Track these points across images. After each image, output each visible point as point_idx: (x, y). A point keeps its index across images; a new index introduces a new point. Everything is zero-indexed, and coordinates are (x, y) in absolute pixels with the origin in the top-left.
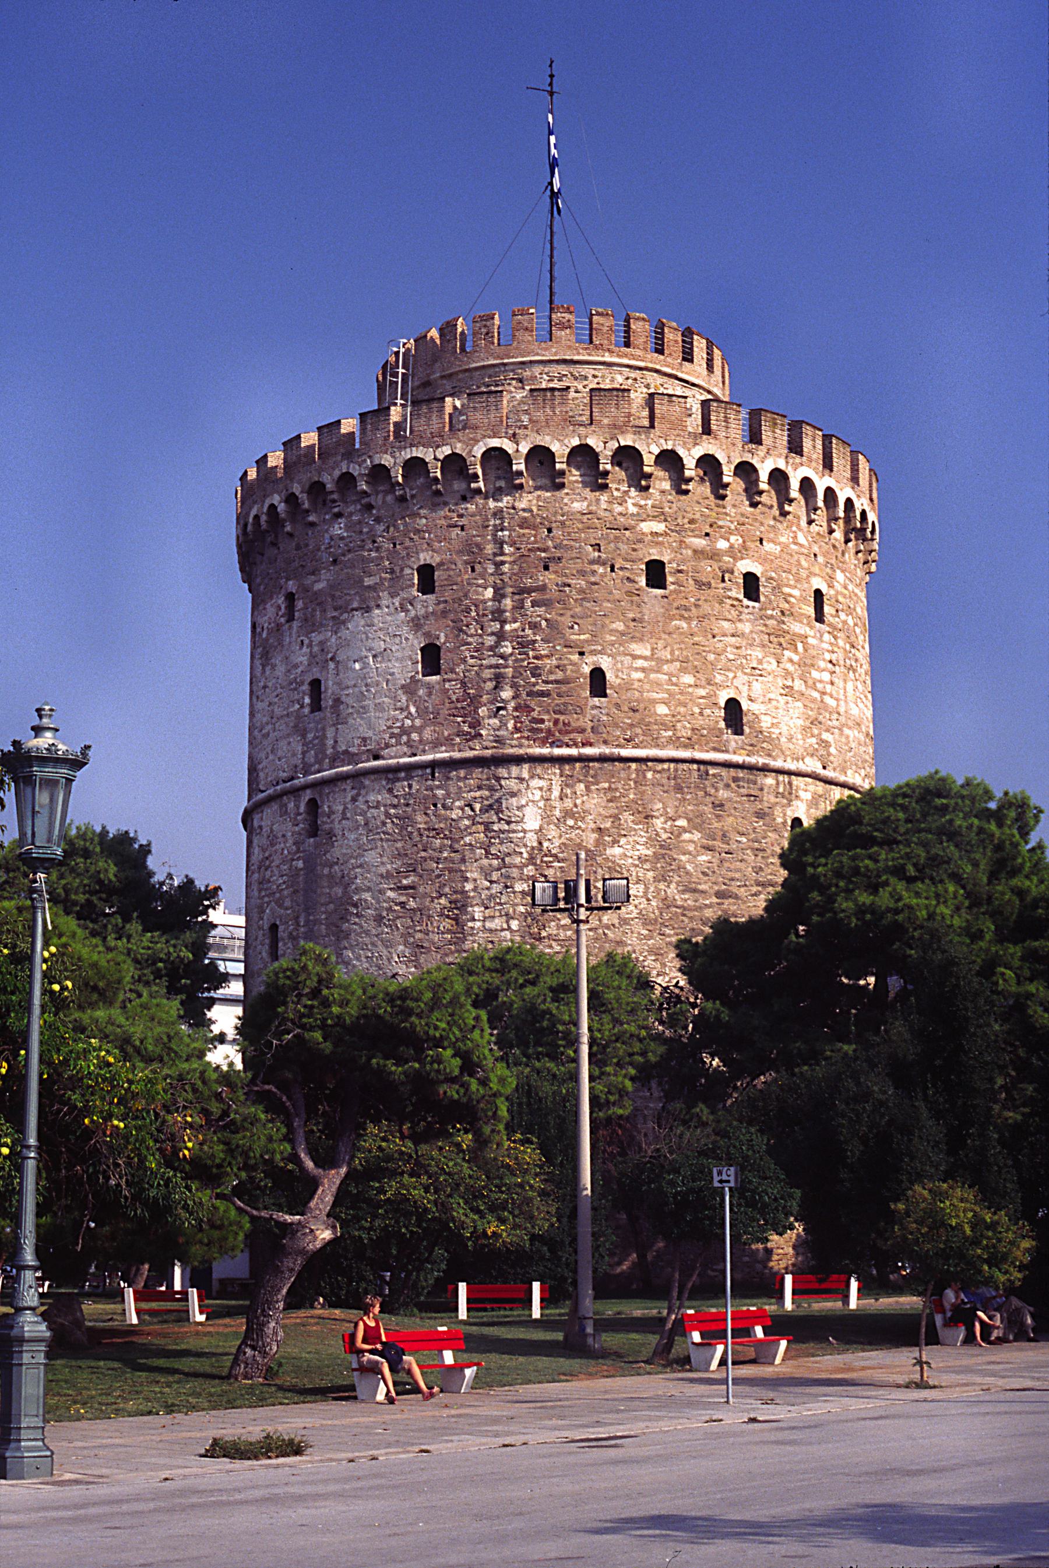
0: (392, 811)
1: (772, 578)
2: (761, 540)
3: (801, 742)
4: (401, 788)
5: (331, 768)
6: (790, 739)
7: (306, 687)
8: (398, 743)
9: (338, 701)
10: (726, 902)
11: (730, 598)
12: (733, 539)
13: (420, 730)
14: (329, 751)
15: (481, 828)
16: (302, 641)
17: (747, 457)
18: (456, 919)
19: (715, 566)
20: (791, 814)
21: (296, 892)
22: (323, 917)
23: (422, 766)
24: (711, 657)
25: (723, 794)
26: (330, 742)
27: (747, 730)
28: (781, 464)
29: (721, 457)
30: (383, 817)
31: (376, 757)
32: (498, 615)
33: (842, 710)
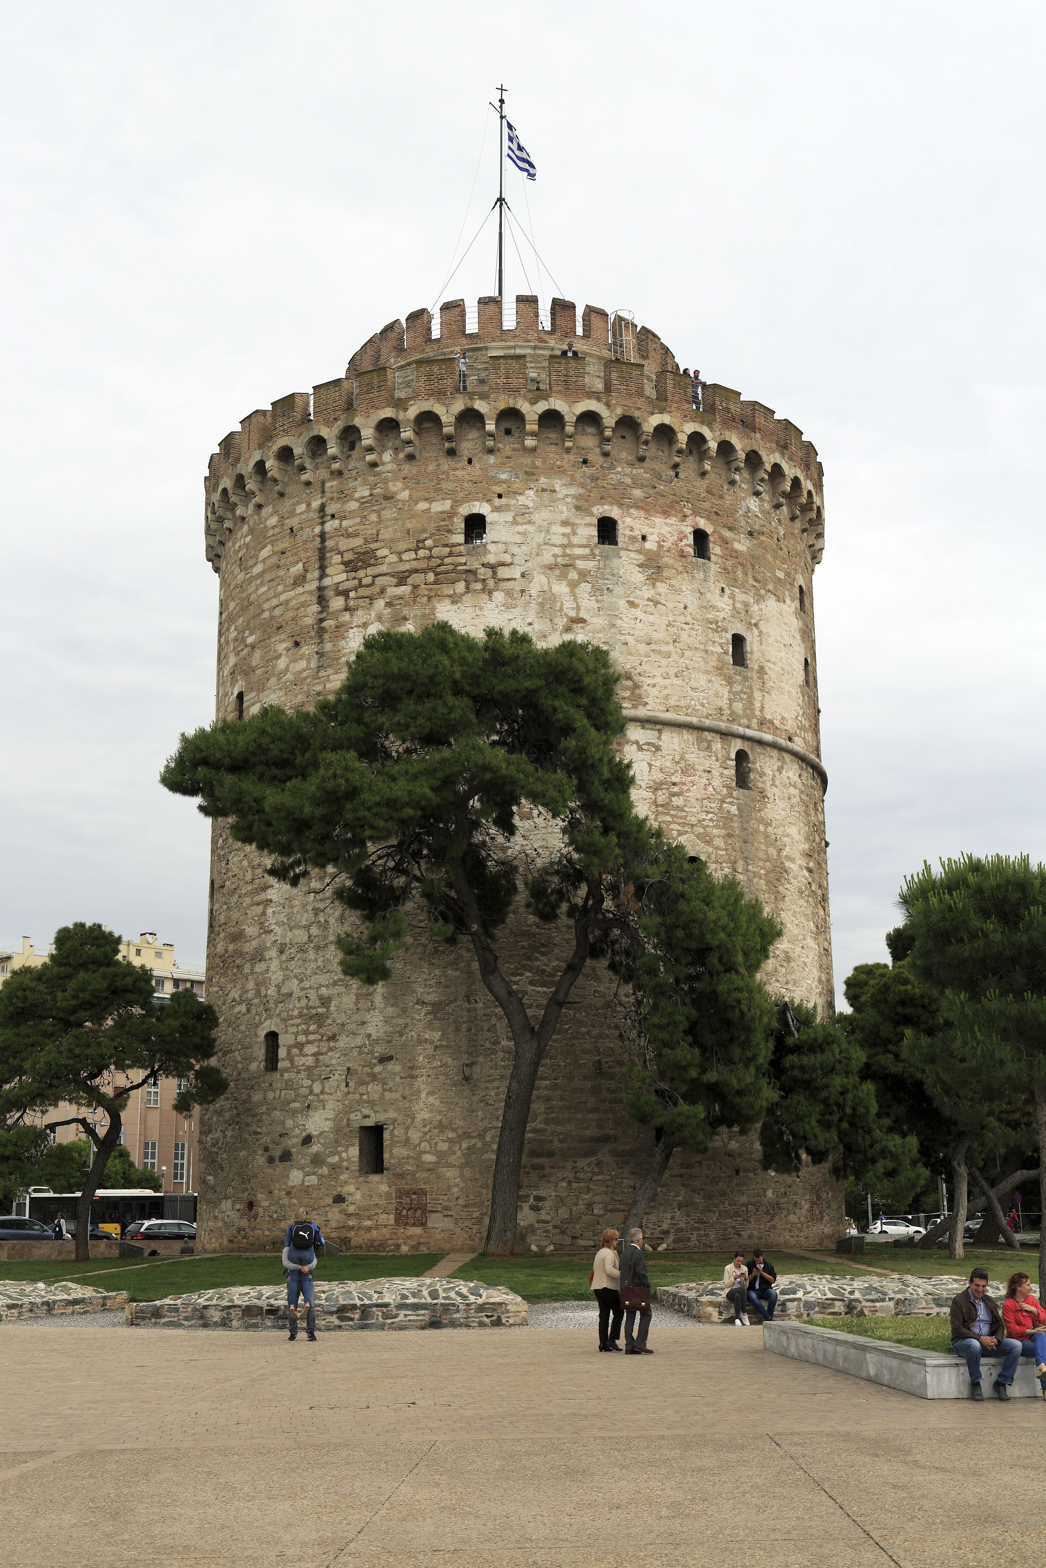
9: (761, 670)
14: (758, 713)
16: (723, 590)
26: (758, 705)
31: (790, 739)
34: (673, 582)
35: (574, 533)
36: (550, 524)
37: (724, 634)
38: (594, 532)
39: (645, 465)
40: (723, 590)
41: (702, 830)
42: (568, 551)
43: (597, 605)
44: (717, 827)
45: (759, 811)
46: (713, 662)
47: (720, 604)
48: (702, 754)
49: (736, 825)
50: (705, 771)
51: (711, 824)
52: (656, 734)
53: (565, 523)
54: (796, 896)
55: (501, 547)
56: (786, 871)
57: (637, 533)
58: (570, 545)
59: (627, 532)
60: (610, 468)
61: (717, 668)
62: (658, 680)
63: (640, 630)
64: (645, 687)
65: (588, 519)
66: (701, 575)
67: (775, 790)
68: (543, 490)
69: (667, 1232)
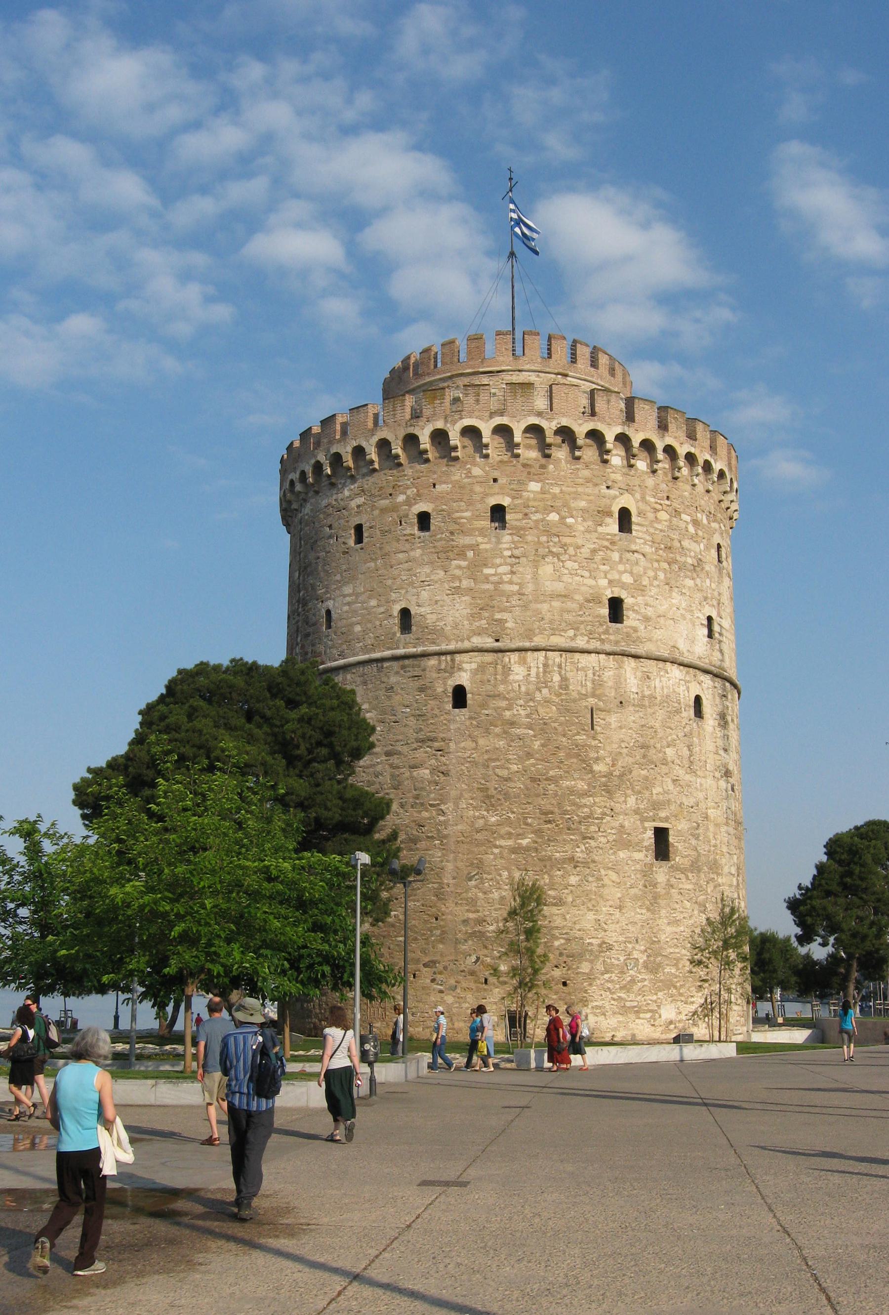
1: (443, 510)
2: (434, 485)
3: (467, 627)
6: (456, 626)
10: (391, 758)
11: (405, 535)
12: (409, 492)
17: (411, 430)
19: (395, 515)
20: (452, 683)
24: (389, 582)
25: (393, 679)
27: (414, 628)
28: (440, 425)
29: (390, 437)
33: (529, 588)
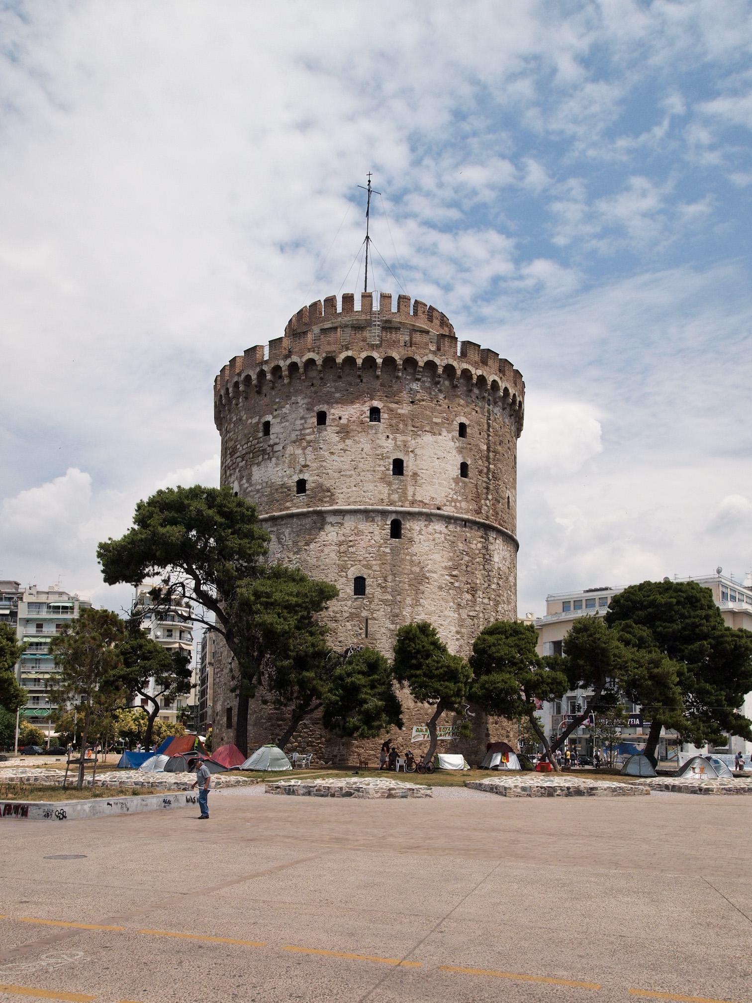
0: (448, 537)
4: (451, 527)
5: (410, 507)
7: (391, 461)
8: (451, 506)
9: (415, 474)
13: (460, 502)
14: (410, 498)
15: (482, 556)
16: (388, 437)
18: (473, 596)
21: (382, 563)
22: (407, 580)
23: (462, 520)
26: (410, 493)
30: (443, 539)
31: (439, 509)
32: (488, 458)
34: (356, 438)
35: (306, 422)
36: (295, 420)
37: (387, 460)
38: (315, 420)
39: (343, 380)
40: (388, 437)
41: (365, 563)
42: (303, 432)
43: (314, 457)
44: (375, 560)
45: (407, 549)
46: (379, 475)
47: (385, 445)
48: (368, 524)
49: (388, 558)
50: (369, 533)
51: (372, 559)
52: (342, 517)
53: (302, 418)
54: (436, 590)
55: (275, 435)
56: (427, 578)
57: (337, 416)
58: (304, 429)
59: (331, 417)
60: (323, 386)
61: (381, 479)
62: (345, 490)
63: (336, 465)
64: (337, 495)
65: (312, 414)
66: (374, 431)
67: (421, 536)
68: (293, 403)
69: (336, 756)
